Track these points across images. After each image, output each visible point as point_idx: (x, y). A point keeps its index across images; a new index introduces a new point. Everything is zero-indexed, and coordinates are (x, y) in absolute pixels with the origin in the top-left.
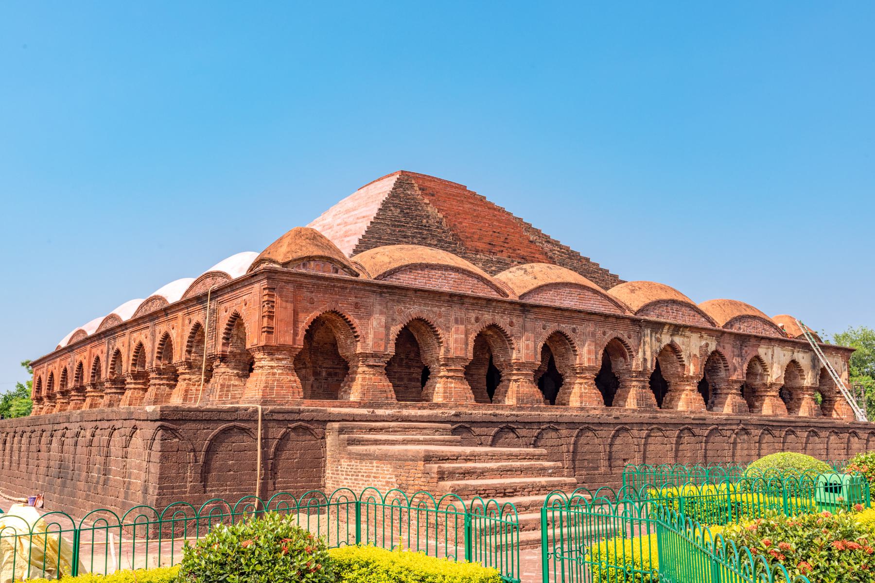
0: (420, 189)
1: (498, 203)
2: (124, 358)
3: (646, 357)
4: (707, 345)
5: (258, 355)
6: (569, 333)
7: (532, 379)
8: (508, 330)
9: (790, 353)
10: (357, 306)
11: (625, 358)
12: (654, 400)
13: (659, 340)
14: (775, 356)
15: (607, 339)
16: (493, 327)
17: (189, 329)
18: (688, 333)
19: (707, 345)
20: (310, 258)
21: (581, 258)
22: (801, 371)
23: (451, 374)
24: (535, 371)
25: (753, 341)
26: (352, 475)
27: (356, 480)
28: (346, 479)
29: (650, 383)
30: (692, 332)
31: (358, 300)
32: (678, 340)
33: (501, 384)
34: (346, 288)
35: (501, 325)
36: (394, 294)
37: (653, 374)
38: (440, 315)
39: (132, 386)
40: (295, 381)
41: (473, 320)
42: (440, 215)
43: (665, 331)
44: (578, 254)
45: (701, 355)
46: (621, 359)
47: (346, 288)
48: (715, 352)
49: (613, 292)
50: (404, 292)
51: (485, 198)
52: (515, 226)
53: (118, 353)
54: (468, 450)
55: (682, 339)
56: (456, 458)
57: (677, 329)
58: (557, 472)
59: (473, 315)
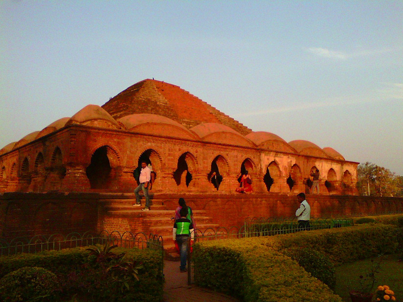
0: (157, 87)
1: (195, 95)
2: (7, 170)
3: (261, 167)
4: (291, 161)
5: (68, 168)
7: (207, 178)
8: (195, 155)
9: (330, 165)
10: (119, 143)
11: (253, 168)
12: (265, 188)
13: (268, 159)
14: (323, 166)
15: (244, 158)
17: (36, 155)
19: (291, 161)
20: (96, 119)
21: (234, 121)
22: (335, 173)
23: (166, 176)
24: (208, 174)
25: (313, 159)
26: (110, 225)
27: (111, 227)
28: (107, 227)
29: (264, 179)
31: (120, 140)
32: (277, 159)
33: (192, 180)
34: (113, 134)
35: (191, 152)
36: (137, 137)
37: (265, 175)
38: (161, 148)
39: (10, 184)
40: (86, 180)
41: (178, 150)
42: (166, 101)
44: (233, 119)
45: (289, 166)
46: (250, 168)
47: (113, 134)
49: (247, 137)
50: (143, 136)
52: (203, 105)
53: (4, 168)
54: (166, 211)
55: (279, 158)
56: (160, 215)
58: (211, 221)
59: (177, 147)
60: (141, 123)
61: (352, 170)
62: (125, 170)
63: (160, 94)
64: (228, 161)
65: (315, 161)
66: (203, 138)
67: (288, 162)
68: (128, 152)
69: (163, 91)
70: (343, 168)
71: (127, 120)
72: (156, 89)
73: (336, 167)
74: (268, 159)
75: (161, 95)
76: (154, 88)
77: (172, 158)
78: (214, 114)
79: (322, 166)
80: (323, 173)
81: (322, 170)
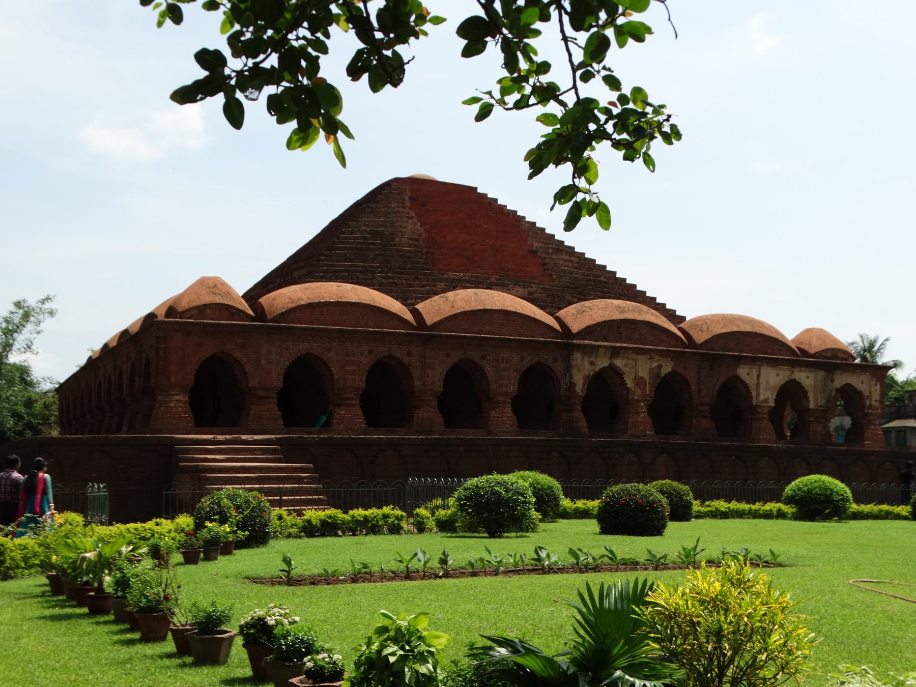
0: (410, 198)
4: (660, 367)
6: (478, 360)
7: (435, 403)
9: (787, 373)
15: (526, 363)
16: (391, 357)
18: (634, 356)
19: (660, 367)
22: (805, 392)
30: (638, 354)
32: (619, 363)
35: (398, 355)
43: (601, 352)
45: (651, 377)
48: (673, 373)
51: (496, 200)
55: (625, 361)
57: (615, 352)
58: (311, 480)
60: (294, 305)
61: (861, 383)
62: (261, 393)
63: (412, 214)
64: (489, 369)
65: (738, 367)
66: (436, 325)
67: (651, 369)
68: (263, 362)
69: (424, 205)
70: (832, 380)
71: (274, 299)
72: (408, 204)
73: (806, 378)
74: (592, 363)
75: (412, 218)
76: (403, 202)
77: (353, 368)
78: (539, 254)
79: (759, 376)
80: (762, 391)
81: (758, 385)
